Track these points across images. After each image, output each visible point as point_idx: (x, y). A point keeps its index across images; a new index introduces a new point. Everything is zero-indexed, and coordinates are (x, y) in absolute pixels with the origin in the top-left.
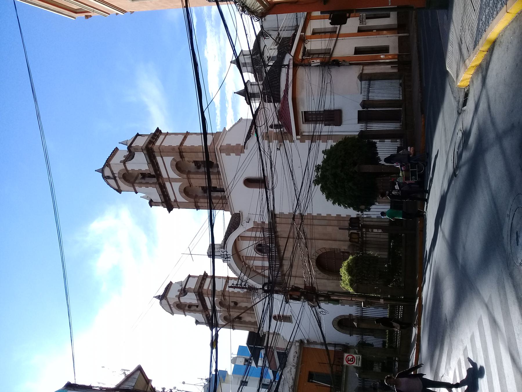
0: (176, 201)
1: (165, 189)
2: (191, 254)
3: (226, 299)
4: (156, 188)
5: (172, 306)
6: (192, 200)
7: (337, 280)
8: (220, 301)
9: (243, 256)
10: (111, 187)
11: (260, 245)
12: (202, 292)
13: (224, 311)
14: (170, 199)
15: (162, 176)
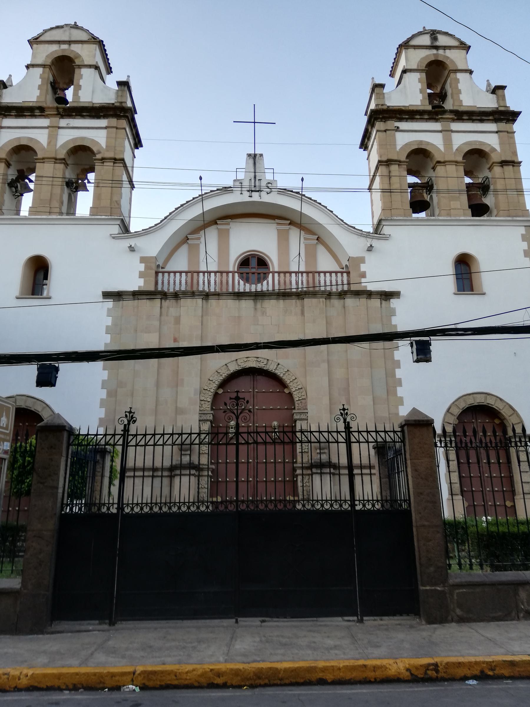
0: (397, 129)
1: (427, 119)
2: (254, 122)
3: (103, 163)
4: (420, 104)
5: (64, 47)
6: (403, 158)
7: (200, 410)
8: (95, 149)
9: (228, 224)
10: (413, 35)
11: (262, 262)
12: (126, 117)
13: (56, 151)
14: (401, 120)
15: (453, 120)
